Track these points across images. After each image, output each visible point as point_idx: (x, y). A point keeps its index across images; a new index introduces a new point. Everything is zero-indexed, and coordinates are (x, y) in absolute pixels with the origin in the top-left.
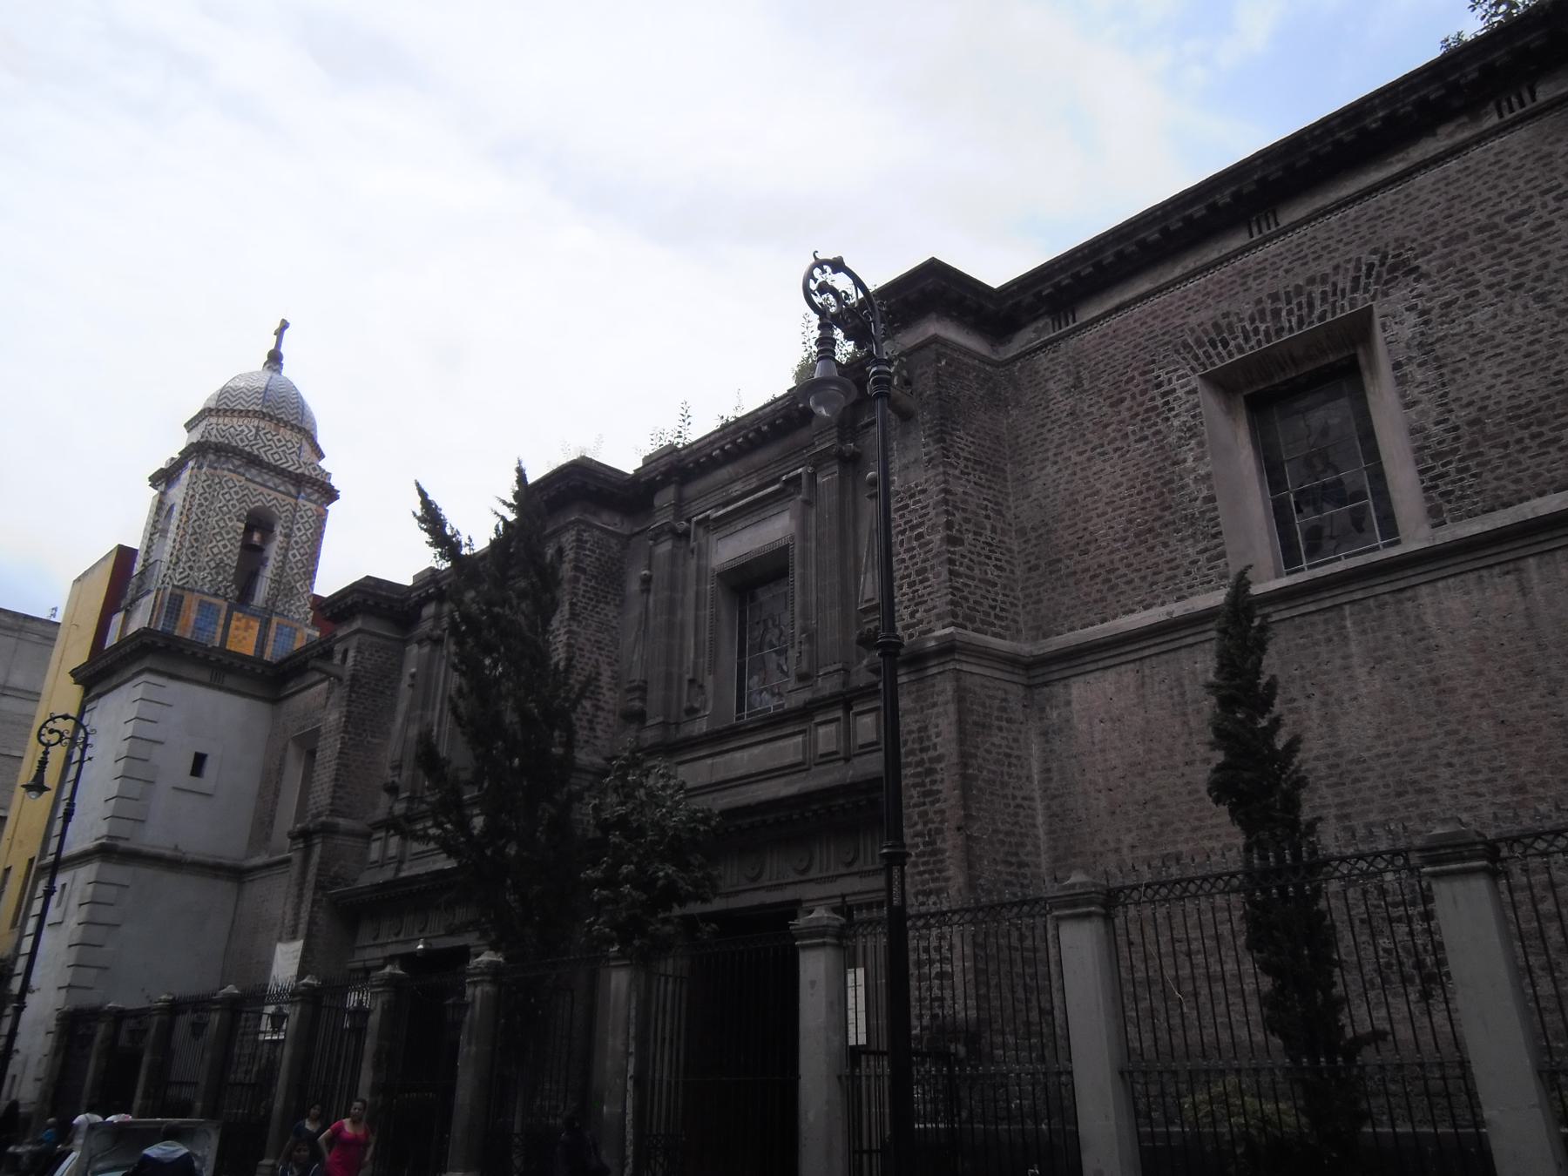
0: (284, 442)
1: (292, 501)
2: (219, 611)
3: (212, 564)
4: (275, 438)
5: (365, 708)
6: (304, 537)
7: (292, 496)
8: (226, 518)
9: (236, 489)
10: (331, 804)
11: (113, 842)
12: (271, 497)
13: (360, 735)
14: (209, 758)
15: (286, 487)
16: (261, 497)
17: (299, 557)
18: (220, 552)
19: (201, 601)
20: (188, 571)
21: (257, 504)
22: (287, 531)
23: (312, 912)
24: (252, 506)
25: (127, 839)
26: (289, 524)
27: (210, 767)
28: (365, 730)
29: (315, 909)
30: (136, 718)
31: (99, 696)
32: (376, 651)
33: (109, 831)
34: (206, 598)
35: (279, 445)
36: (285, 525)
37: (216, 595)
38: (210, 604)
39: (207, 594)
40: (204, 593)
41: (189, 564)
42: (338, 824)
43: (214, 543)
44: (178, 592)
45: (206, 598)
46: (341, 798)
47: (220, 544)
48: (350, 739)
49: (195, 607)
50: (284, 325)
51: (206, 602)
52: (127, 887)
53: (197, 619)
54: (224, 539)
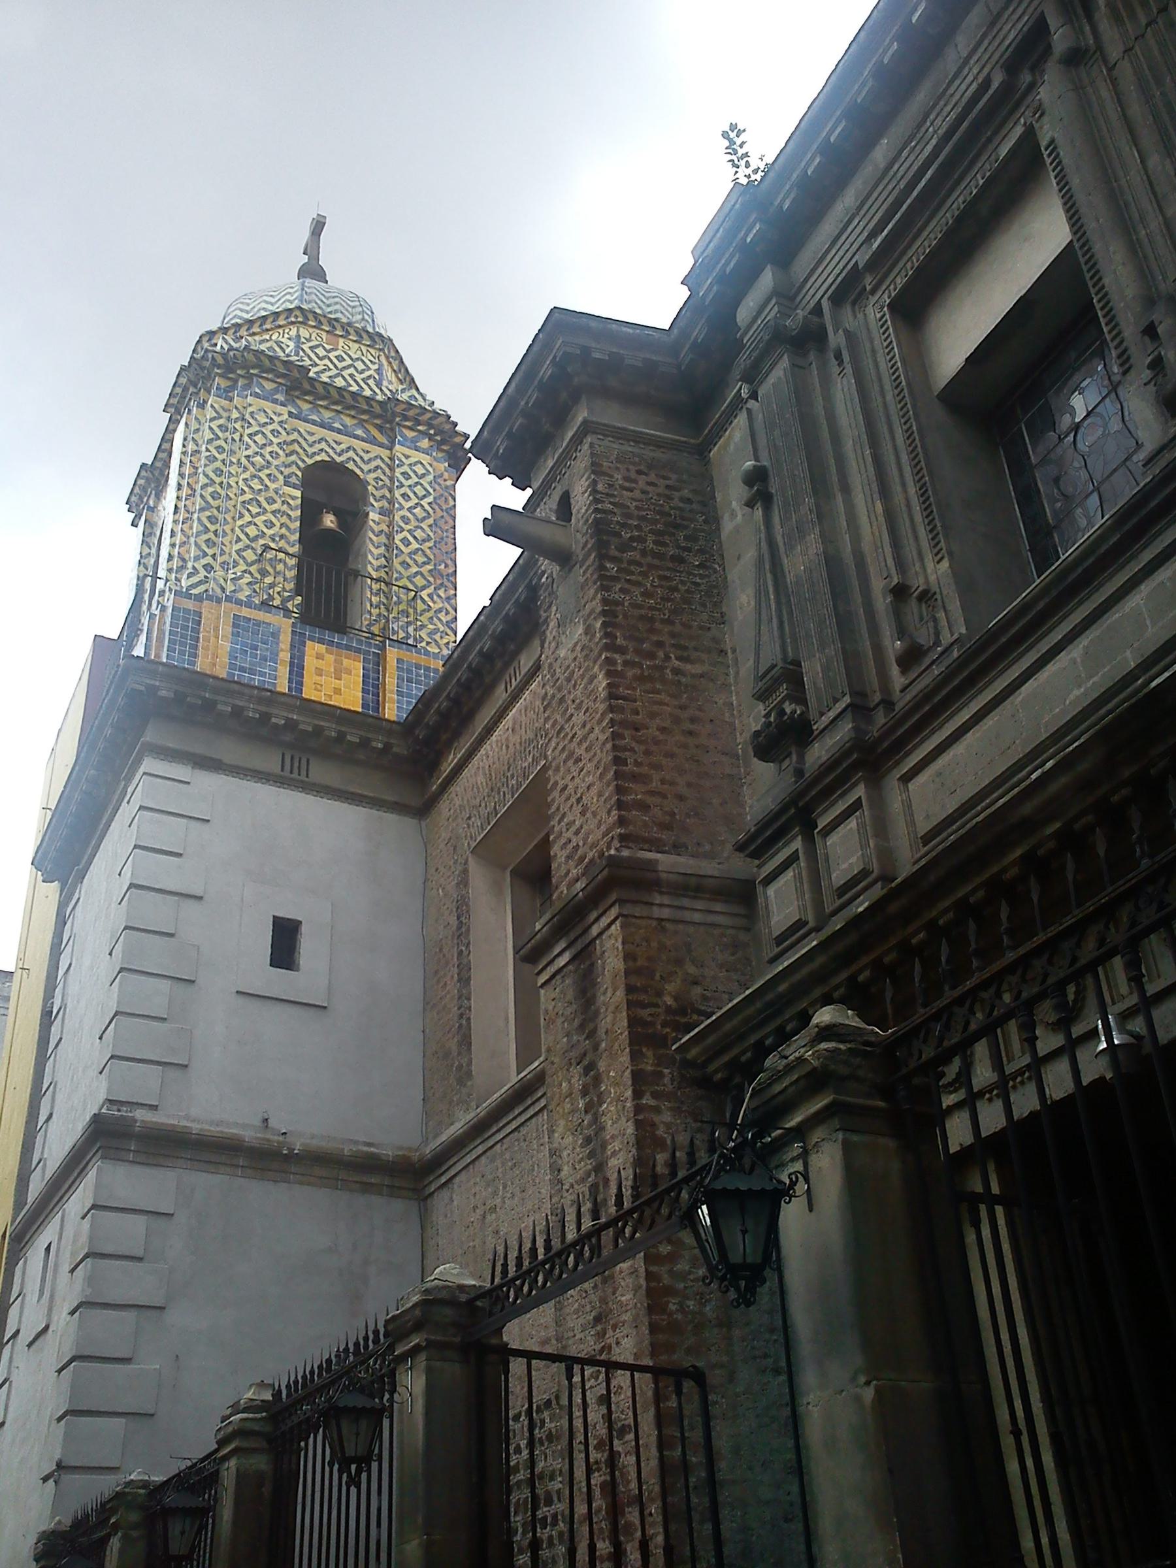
1: (385, 453)
2: (275, 635)
3: (250, 555)
4: (332, 355)
5: (647, 594)
7: (381, 445)
8: (262, 475)
10: (621, 822)
11: (124, 1112)
13: (651, 656)
15: (367, 431)
16: (323, 445)
17: (415, 545)
20: (203, 573)
21: (318, 458)
23: (638, 1109)
24: (310, 462)
25: (154, 1108)
27: (308, 947)
28: (660, 644)
29: (647, 1100)
32: (639, 472)
34: (245, 612)
35: (340, 365)
37: (265, 605)
38: (258, 623)
39: (249, 605)
40: (239, 602)
41: (204, 561)
42: (652, 863)
43: (248, 518)
44: (190, 605)
45: (245, 612)
48: (626, 663)
49: (226, 629)
53: (233, 650)
54: (265, 511)
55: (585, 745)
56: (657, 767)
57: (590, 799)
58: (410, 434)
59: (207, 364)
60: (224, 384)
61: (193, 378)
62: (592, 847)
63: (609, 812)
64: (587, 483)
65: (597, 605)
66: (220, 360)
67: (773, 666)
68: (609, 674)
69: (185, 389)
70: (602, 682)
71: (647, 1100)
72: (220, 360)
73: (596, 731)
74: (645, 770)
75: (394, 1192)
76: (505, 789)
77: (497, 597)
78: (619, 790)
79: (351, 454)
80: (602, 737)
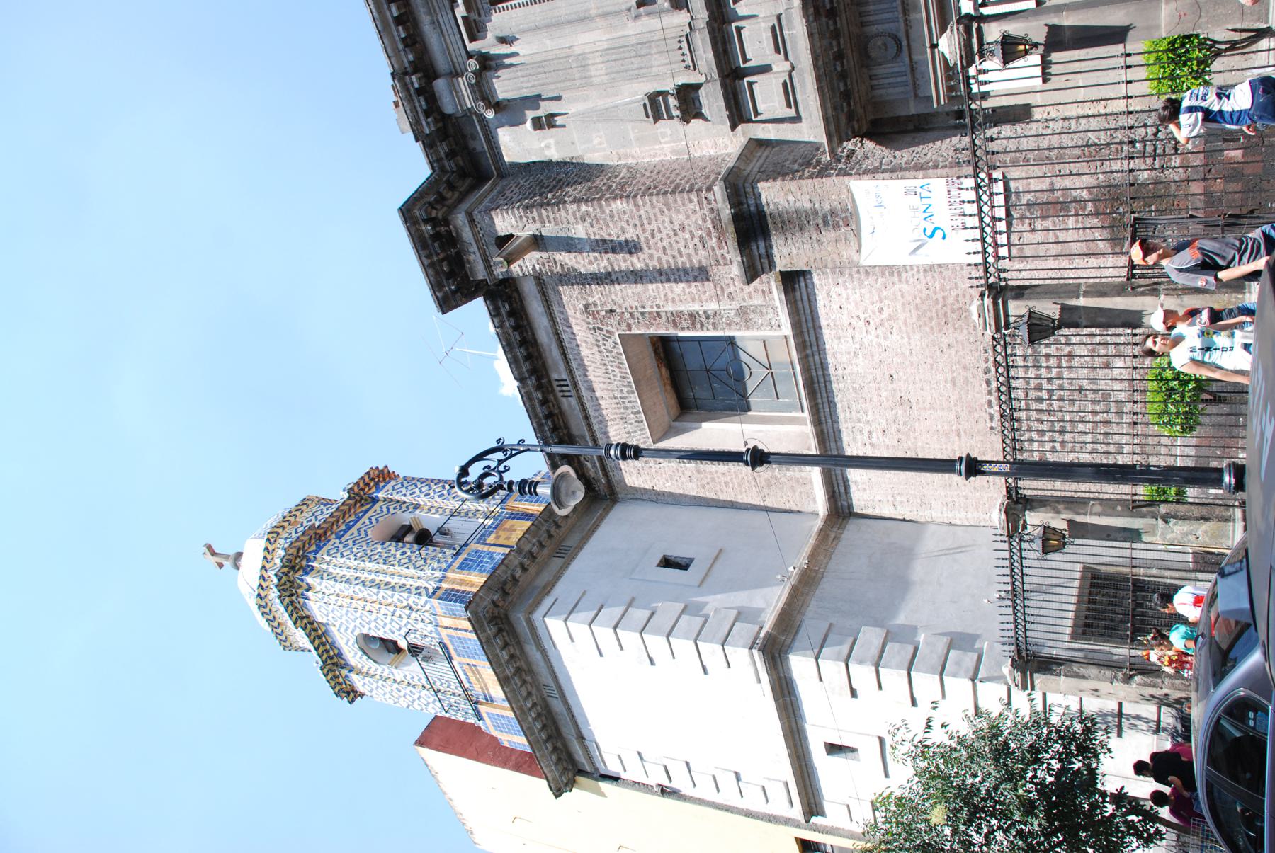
0: (313, 518)
2: (477, 552)
6: (423, 489)
9: (341, 546)
12: (367, 522)
13: (610, 187)
14: (668, 553)
16: (362, 530)
17: (445, 492)
18: (409, 558)
19: (459, 568)
22: (411, 507)
26: (404, 506)
27: (678, 552)
30: (590, 625)
31: (590, 758)
33: (744, 647)
36: (404, 509)
45: (457, 564)
46: (692, 185)
47: (398, 556)
50: (209, 548)
51: (462, 564)
52: (831, 625)
55: (647, 226)
56: (672, 182)
57: (679, 219)
58: (374, 490)
59: (284, 579)
60: (301, 572)
61: (288, 594)
62: (704, 221)
63: (691, 201)
64: (500, 216)
65: (572, 208)
66: (285, 570)
67: (645, 105)
68: (614, 199)
69: (292, 602)
70: (619, 205)
71: (853, 172)
72: (285, 570)
73: (642, 212)
74: (673, 186)
75: (842, 527)
76: (626, 401)
77: (516, 373)
78: (682, 191)
79: (373, 519)
80: (648, 207)
